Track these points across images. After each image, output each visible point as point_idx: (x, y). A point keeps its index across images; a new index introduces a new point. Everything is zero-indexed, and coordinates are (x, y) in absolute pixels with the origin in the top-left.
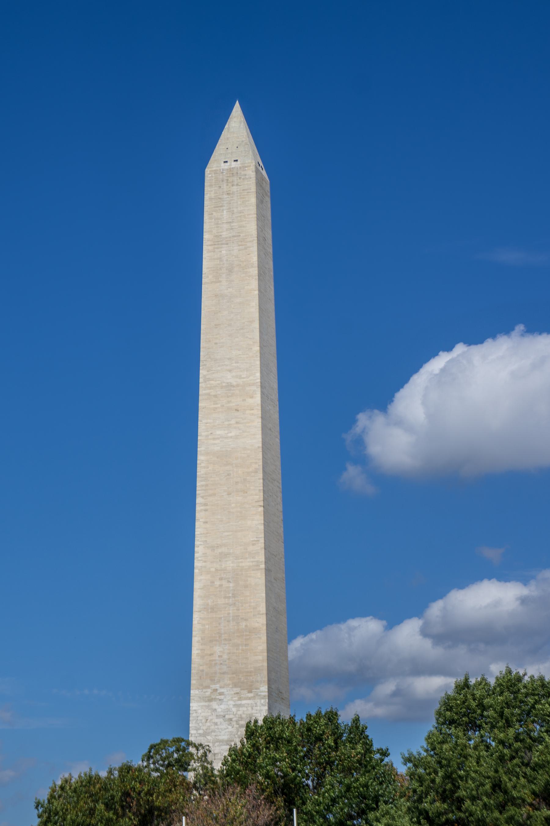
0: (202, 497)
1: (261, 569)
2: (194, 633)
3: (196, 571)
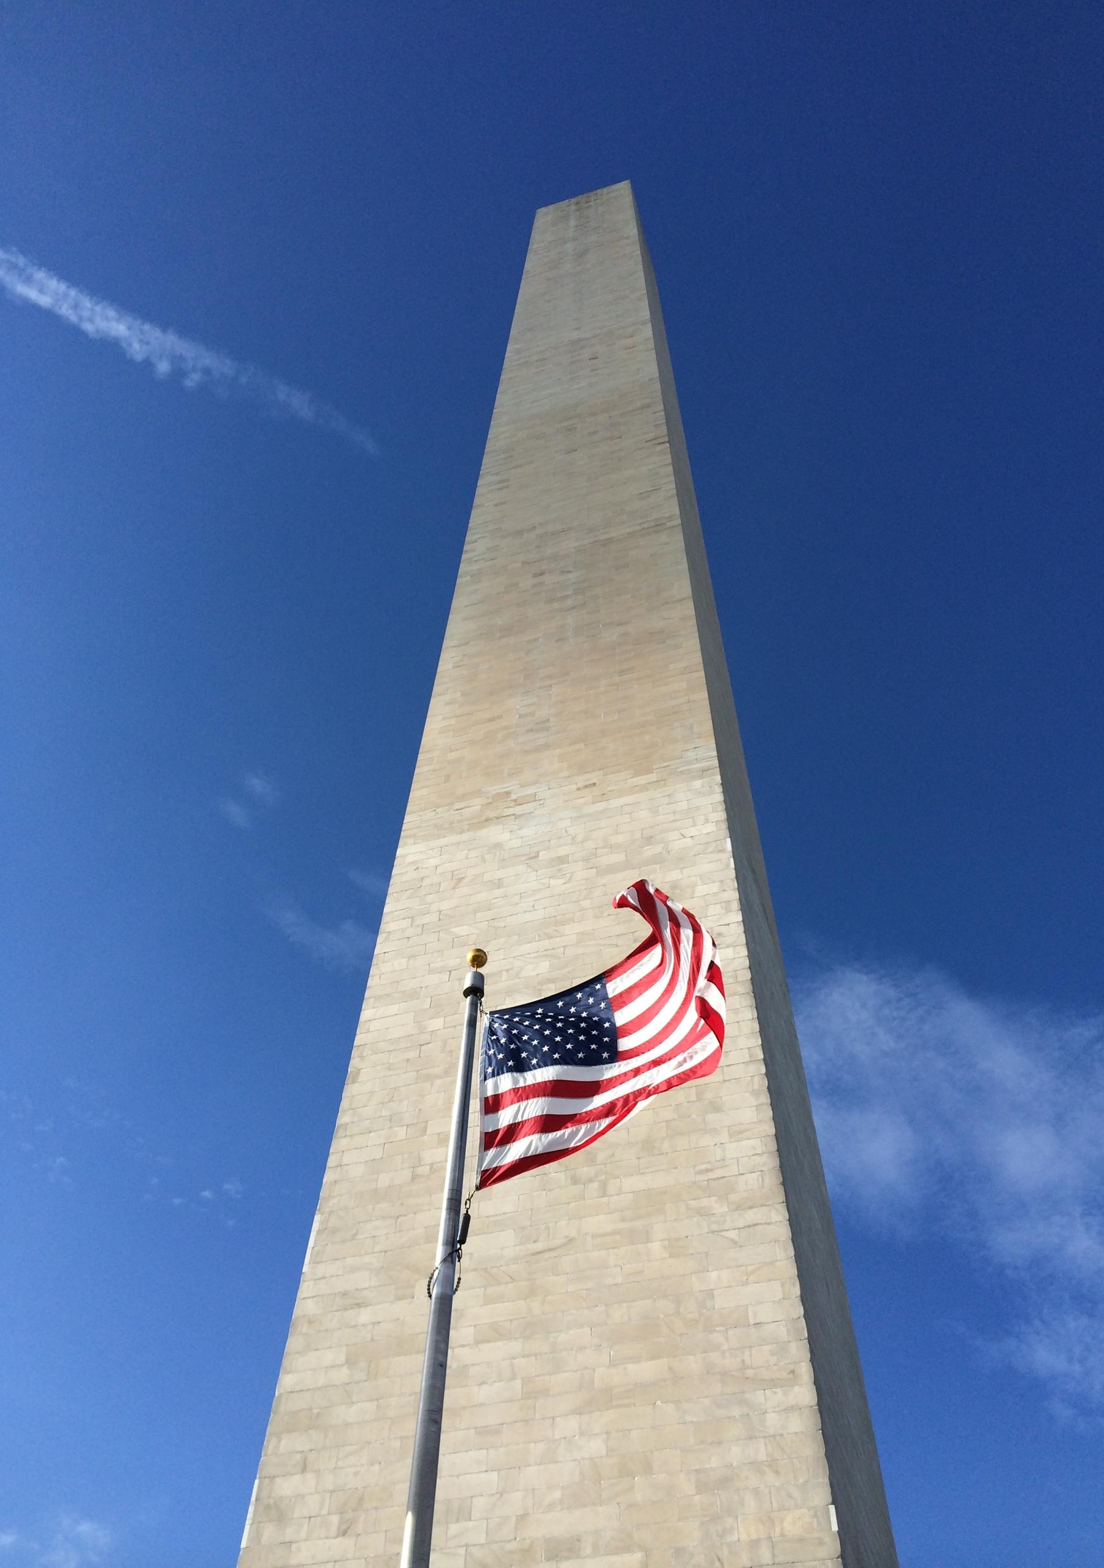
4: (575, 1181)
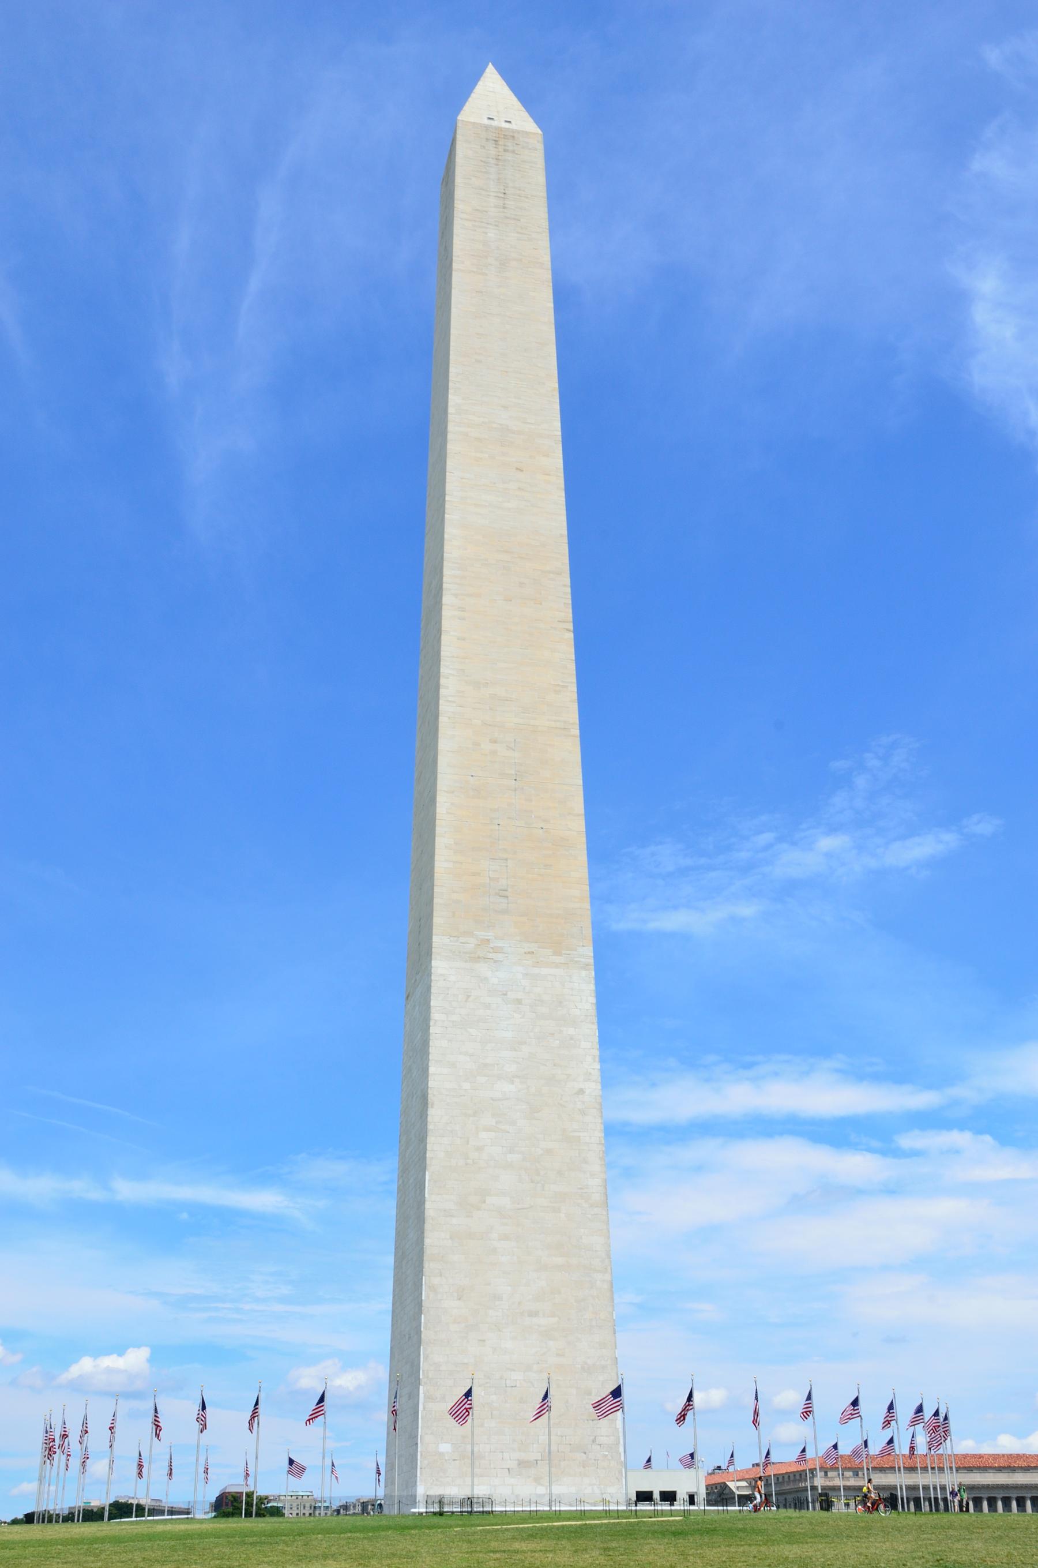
0: (456, 595)
1: (574, 736)
2: (439, 830)
3: (443, 719)
4: (532, 1182)
